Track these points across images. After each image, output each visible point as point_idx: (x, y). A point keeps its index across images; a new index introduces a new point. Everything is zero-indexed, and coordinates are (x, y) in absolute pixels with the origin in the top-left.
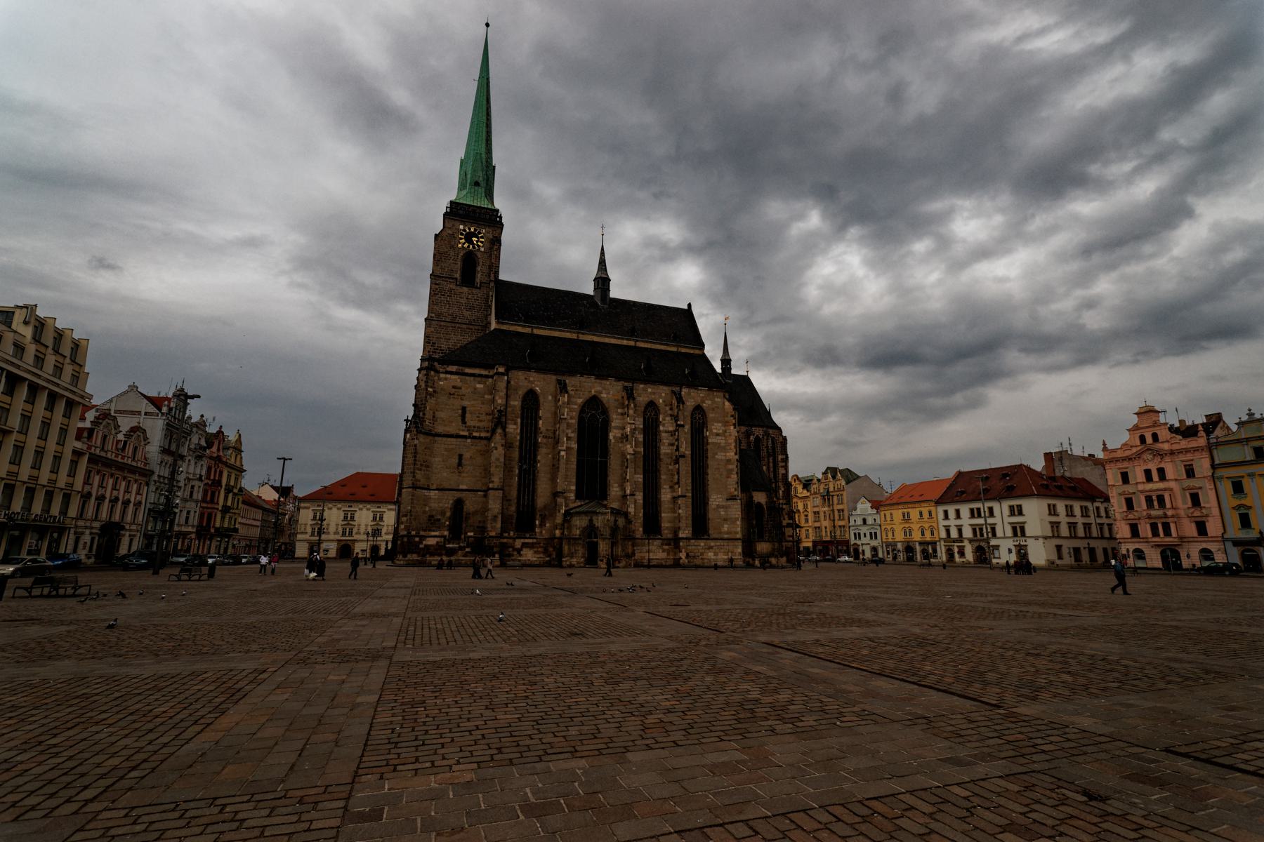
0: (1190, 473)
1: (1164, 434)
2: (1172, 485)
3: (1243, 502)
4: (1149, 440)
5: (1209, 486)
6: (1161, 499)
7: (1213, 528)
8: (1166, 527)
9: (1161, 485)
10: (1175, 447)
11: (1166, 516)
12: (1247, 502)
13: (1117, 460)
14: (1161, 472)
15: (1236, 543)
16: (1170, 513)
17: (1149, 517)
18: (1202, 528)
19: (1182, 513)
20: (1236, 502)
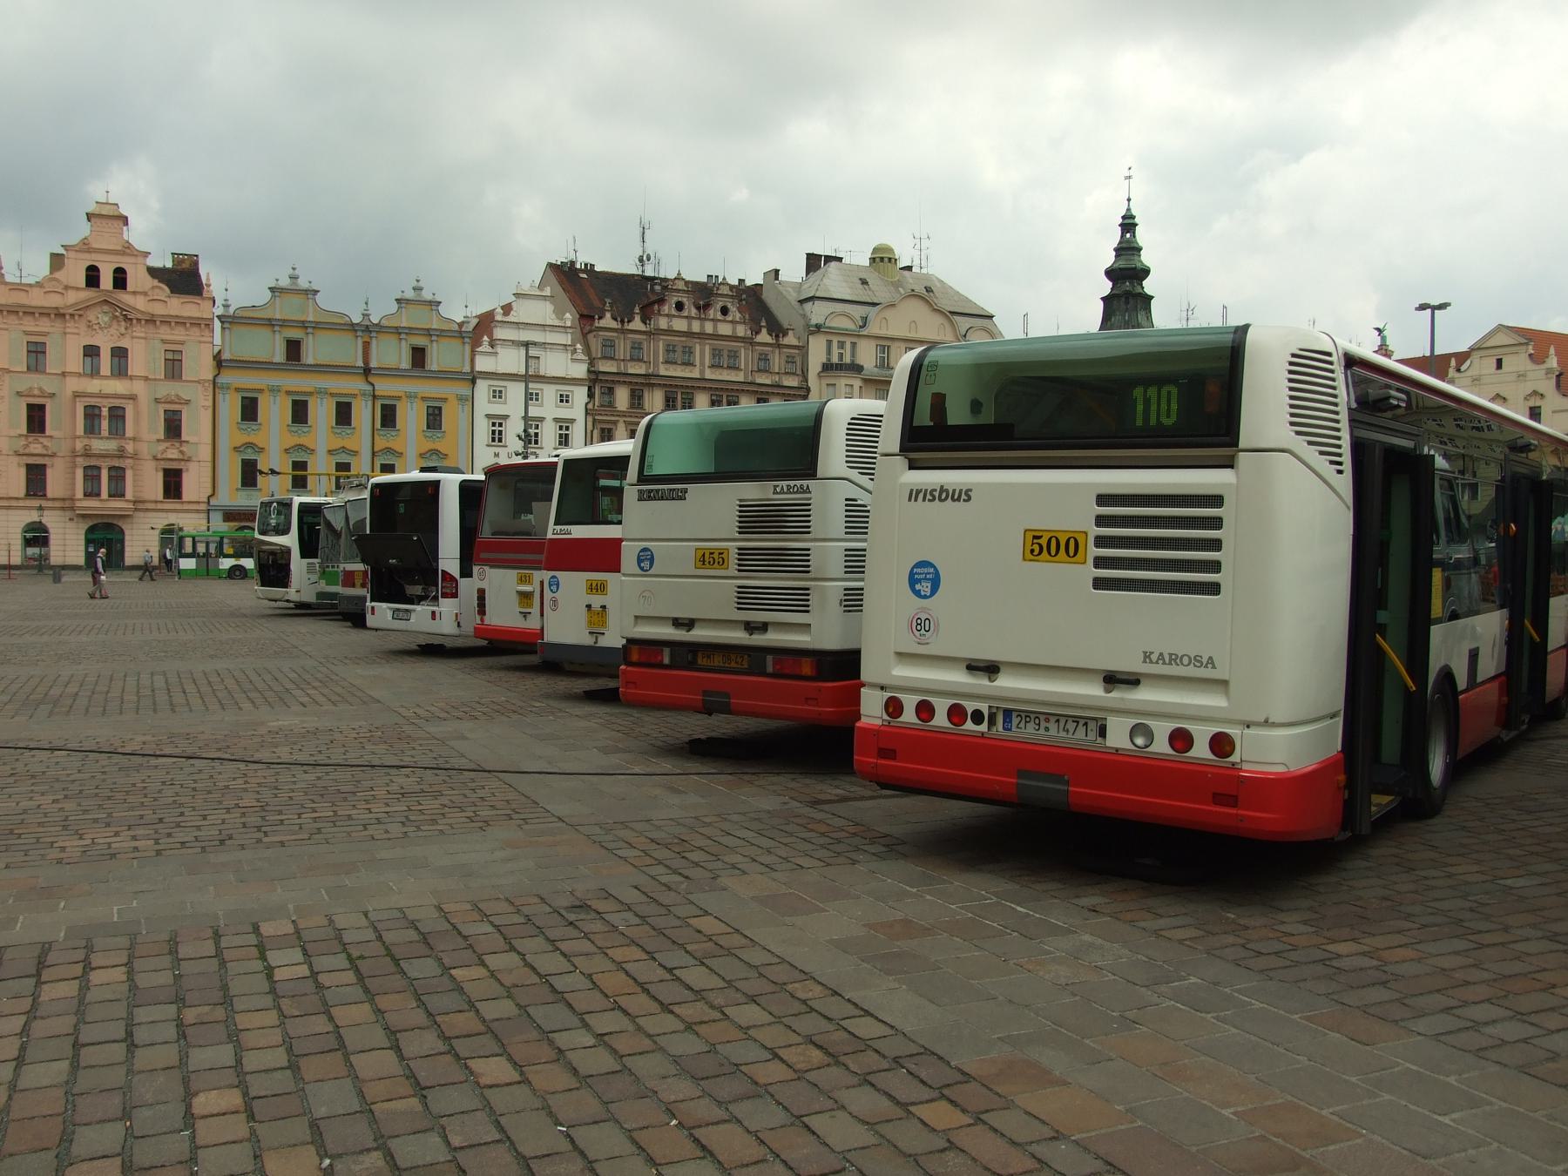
0: (174, 367)
1: (137, 278)
2: (138, 388)
3: (252, 439)
4: (107, 281)
5: (202, 398)
6: (117, 415)
7: (195, 484)
8: (118, 475)
9: (118, 386)
10: (158, 309)
11: (121, 454)
12: (257, 439)
13: (30, 312)
14: (120, 354)
15: (229, 516)
16: (130, 448)
17: (87, 454)
18: (173, 484)
19: (145, 450)
20: (242, 439)
